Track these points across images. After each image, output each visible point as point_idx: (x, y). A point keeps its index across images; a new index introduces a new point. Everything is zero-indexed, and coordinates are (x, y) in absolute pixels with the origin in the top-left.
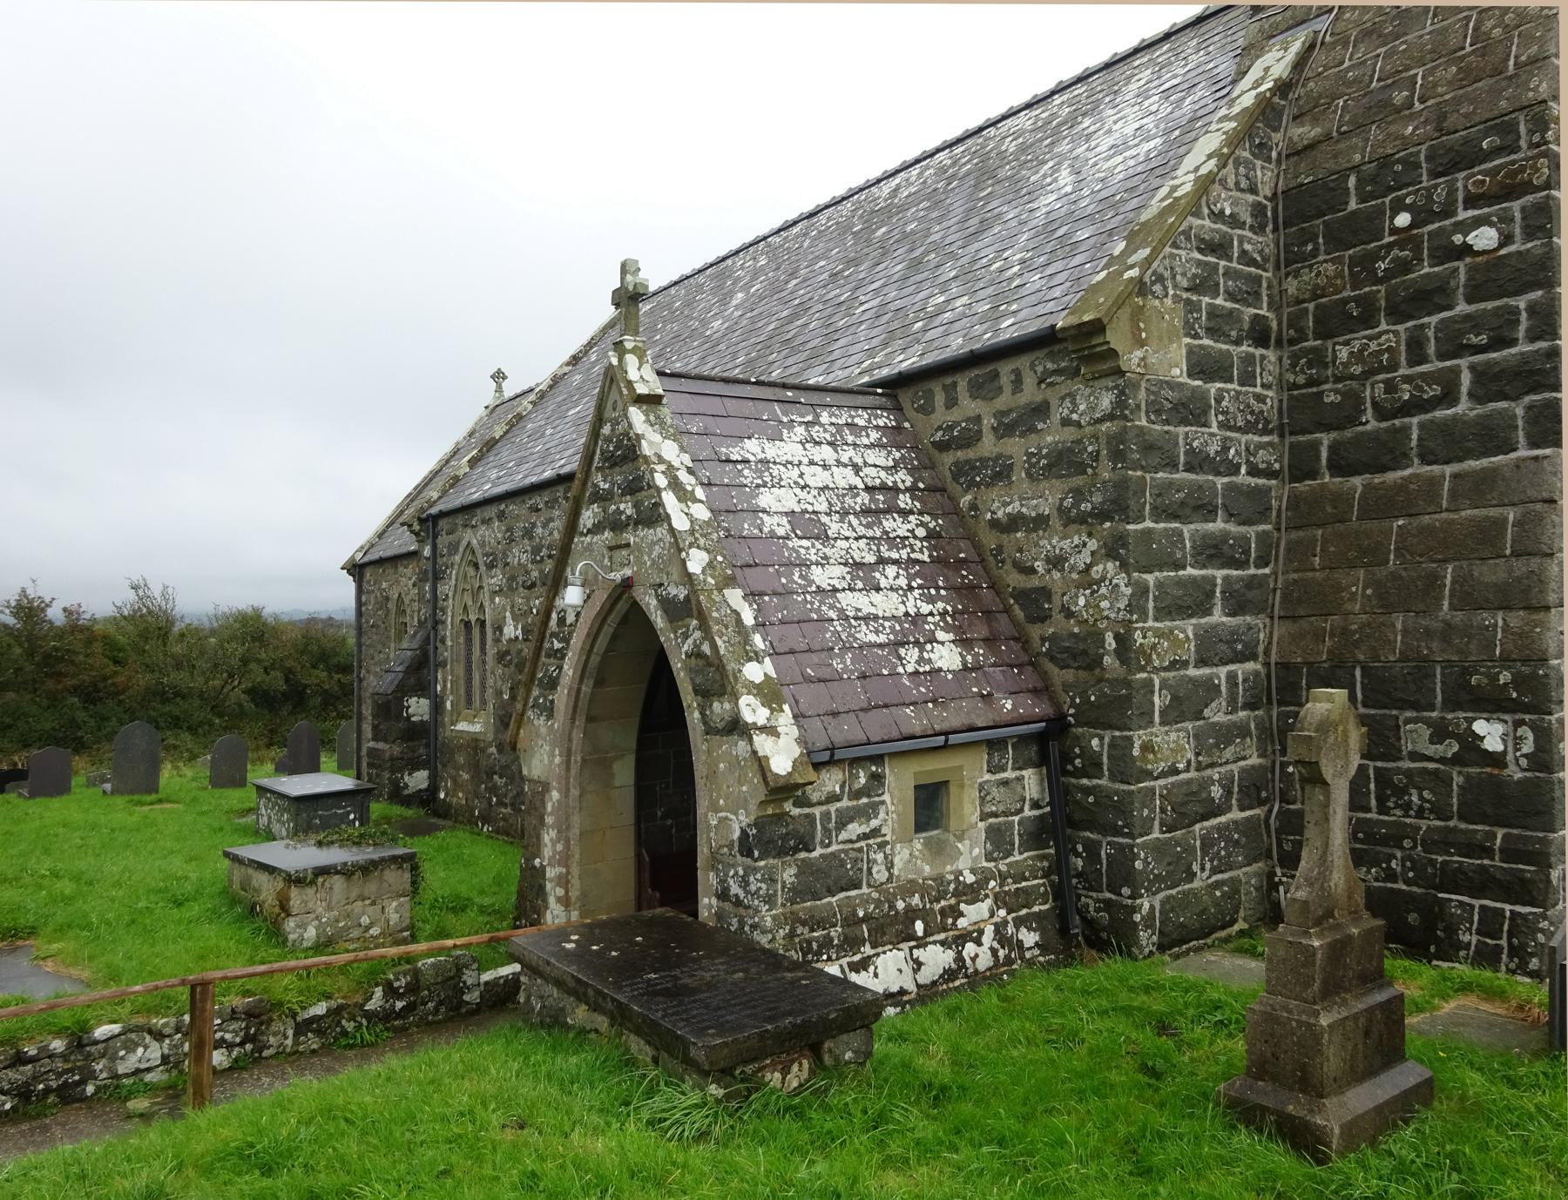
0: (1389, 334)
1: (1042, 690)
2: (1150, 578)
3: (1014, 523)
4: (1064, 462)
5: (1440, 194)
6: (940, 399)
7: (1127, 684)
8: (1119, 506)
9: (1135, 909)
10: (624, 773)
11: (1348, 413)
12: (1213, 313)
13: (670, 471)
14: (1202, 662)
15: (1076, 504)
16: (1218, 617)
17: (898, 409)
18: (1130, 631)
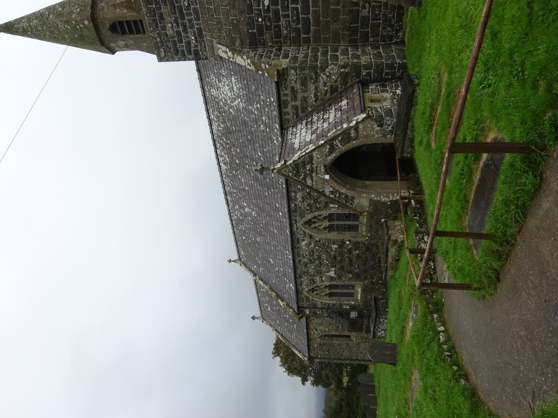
0: (283, 22)
1: (352, 86)
2: (330, 63)
3: (316, 95)
4: (304, 83)
5: (256, 12)
6: (287, 117)
7: (352, 66)
8: (314, 68)
9: (399, 63)
10: (368, 183)
11: (297, 31)
12: (275, 55)
13: (301, 153)
14: (348, 55)
15: (313, 79)
16: (339, 54)
17: (288, 128)
18: (341, 65)
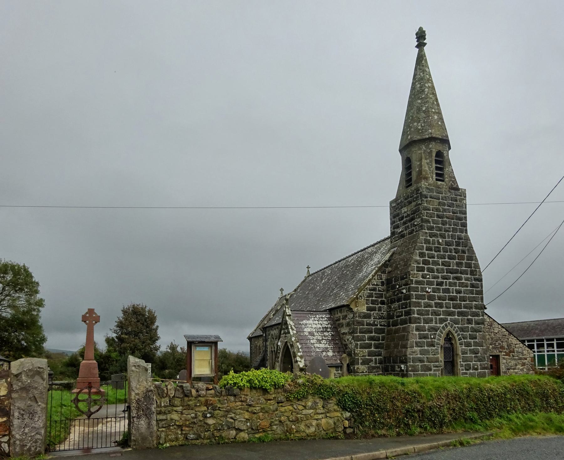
2: (359, 343)
